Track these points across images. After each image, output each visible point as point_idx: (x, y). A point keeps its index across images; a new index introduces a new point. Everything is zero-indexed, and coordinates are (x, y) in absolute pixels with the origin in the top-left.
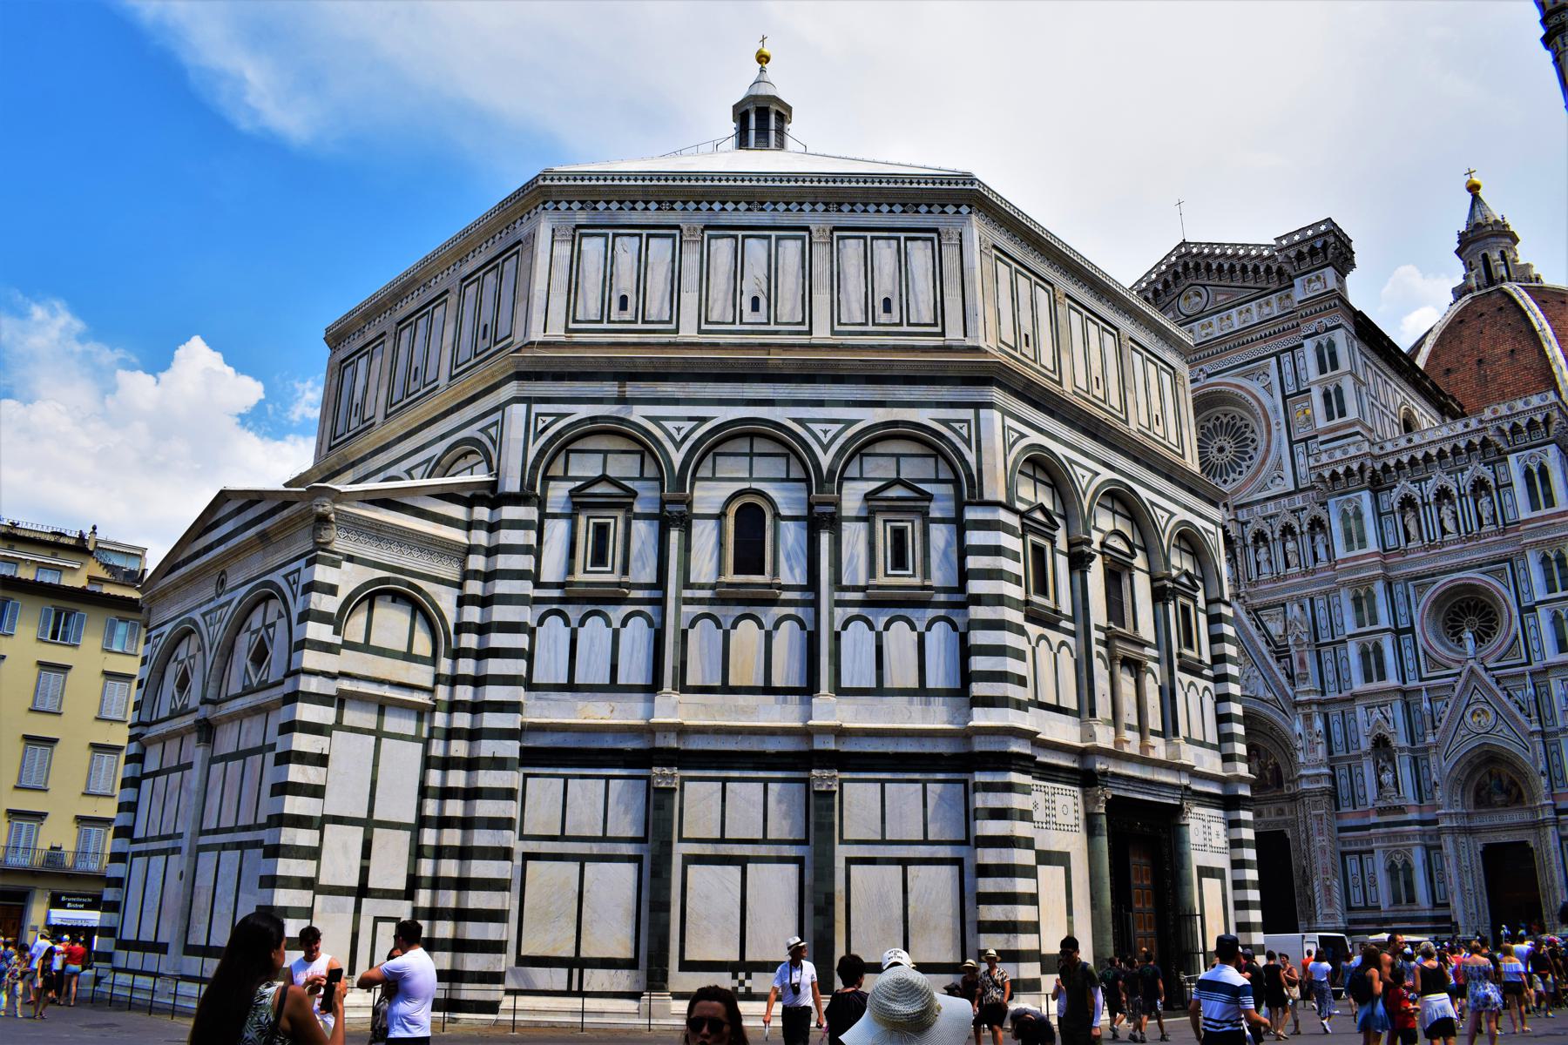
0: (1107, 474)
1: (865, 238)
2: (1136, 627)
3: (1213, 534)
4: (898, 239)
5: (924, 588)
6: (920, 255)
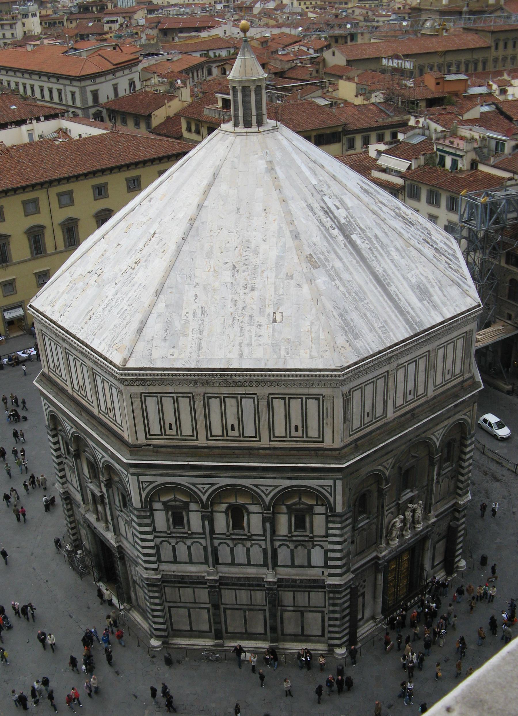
4: (302, 399)
6: (313, 405)
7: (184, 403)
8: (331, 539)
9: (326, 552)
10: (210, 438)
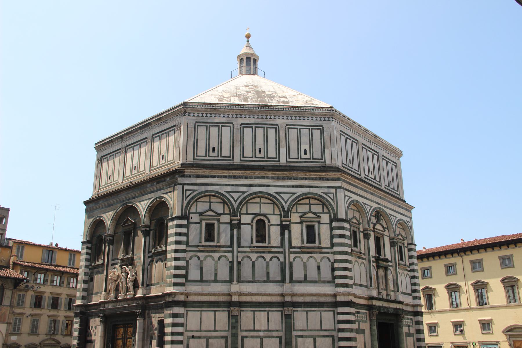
0: (375, 205)
1: (297, 128)
2: (385, 256)
3: (409, 222)
5: (319, 248)
7: (226, 131)
8: (336, 249)
9: (333, 264)
10: (242, 159)
